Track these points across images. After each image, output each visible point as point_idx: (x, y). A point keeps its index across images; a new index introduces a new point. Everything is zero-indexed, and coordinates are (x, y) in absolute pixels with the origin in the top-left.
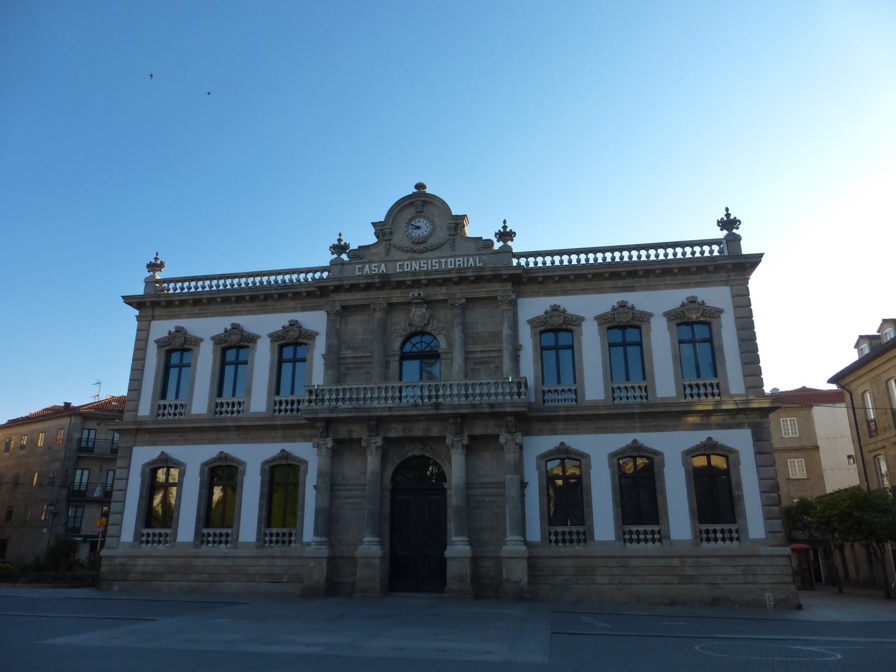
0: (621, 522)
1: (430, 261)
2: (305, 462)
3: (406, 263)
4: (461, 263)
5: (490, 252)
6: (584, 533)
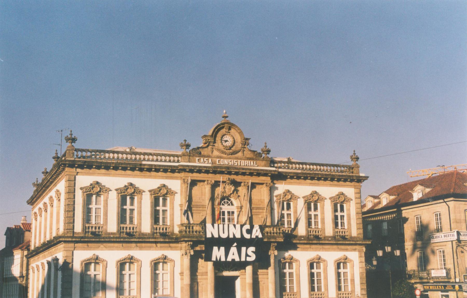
3: (221, 160)
4: (248, 163)
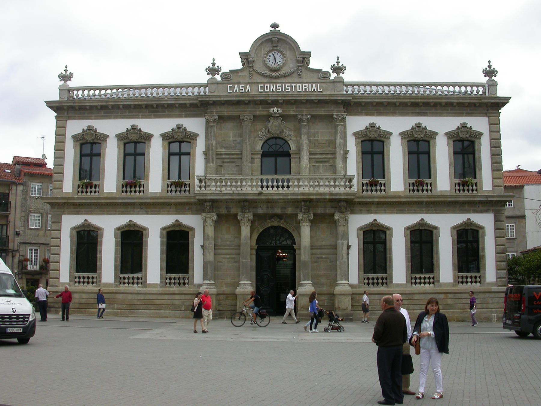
0: (410, 272)
1: (283, 85)
2: (193, 229)
3: (266, 85)
4: (307, 88)
5: (328, 81)
6: (386, 279)
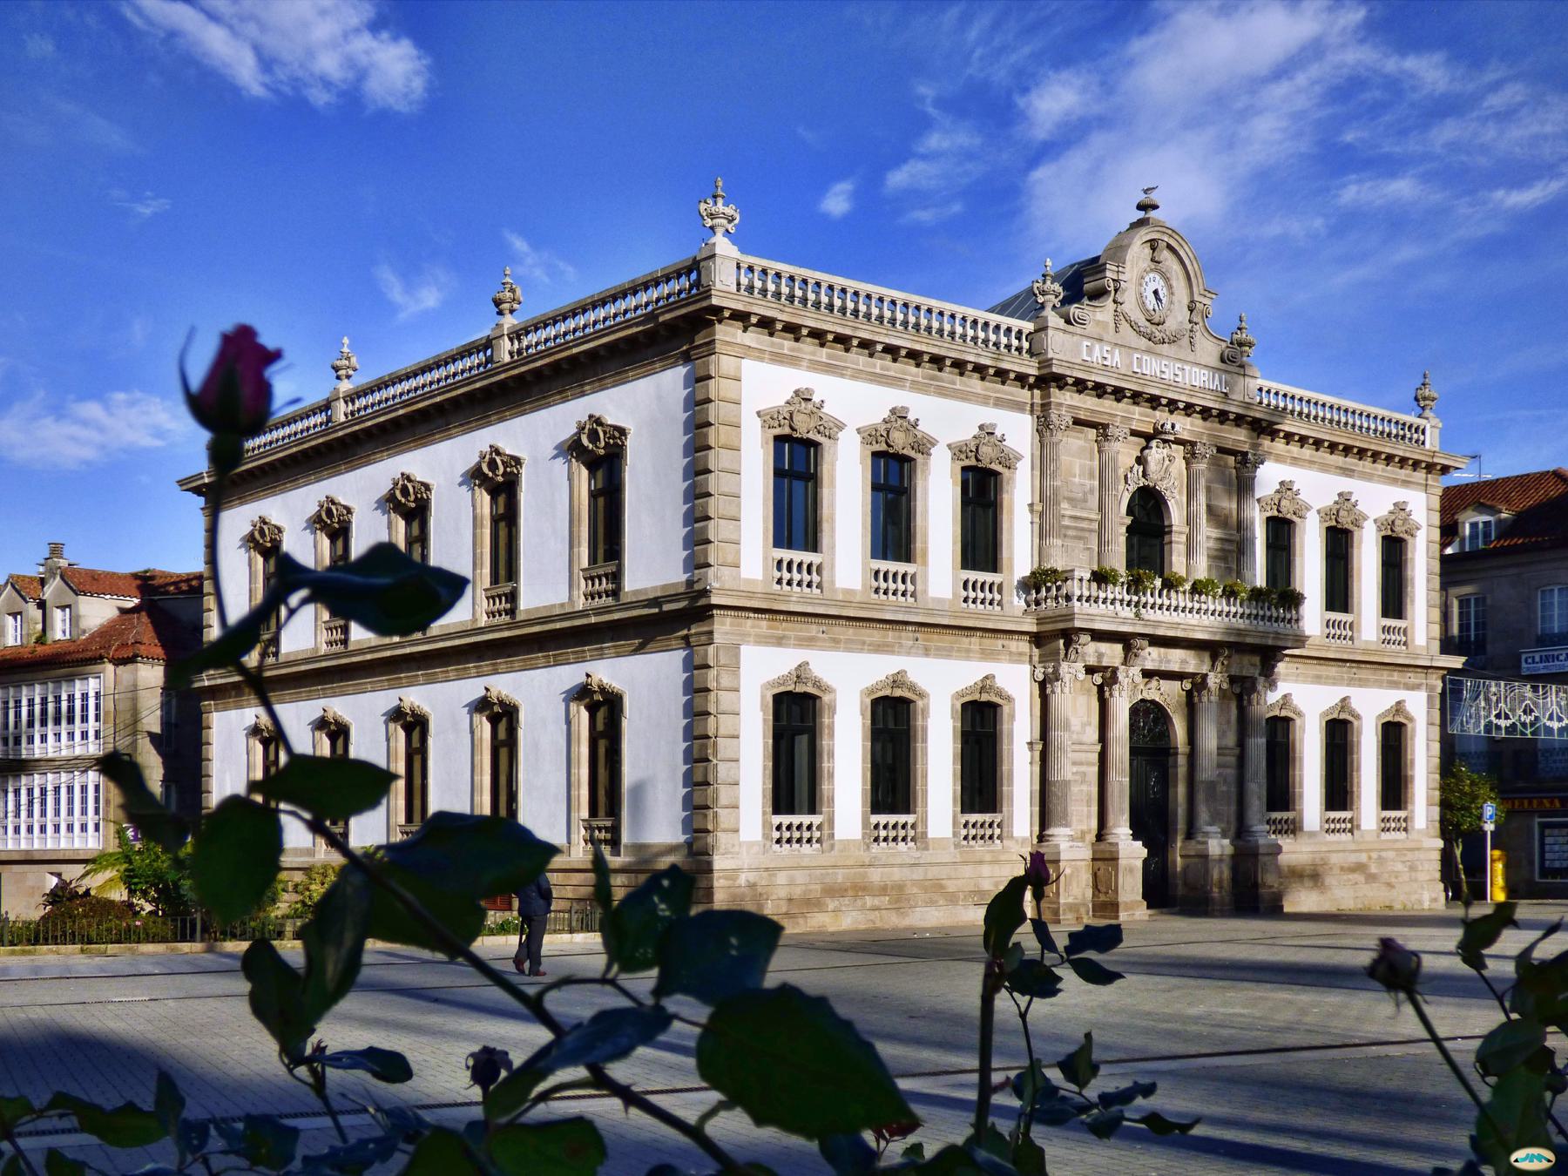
4: (1206, 379)
